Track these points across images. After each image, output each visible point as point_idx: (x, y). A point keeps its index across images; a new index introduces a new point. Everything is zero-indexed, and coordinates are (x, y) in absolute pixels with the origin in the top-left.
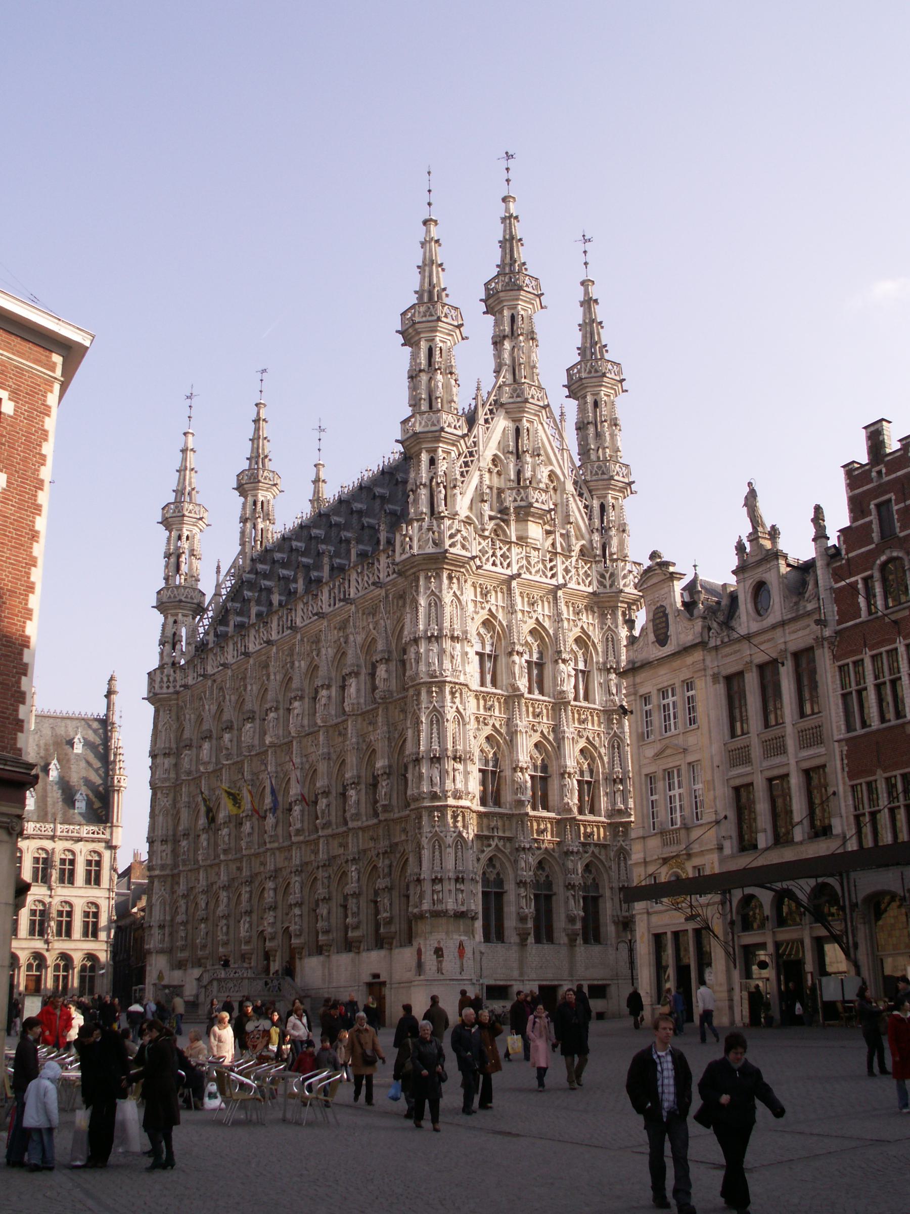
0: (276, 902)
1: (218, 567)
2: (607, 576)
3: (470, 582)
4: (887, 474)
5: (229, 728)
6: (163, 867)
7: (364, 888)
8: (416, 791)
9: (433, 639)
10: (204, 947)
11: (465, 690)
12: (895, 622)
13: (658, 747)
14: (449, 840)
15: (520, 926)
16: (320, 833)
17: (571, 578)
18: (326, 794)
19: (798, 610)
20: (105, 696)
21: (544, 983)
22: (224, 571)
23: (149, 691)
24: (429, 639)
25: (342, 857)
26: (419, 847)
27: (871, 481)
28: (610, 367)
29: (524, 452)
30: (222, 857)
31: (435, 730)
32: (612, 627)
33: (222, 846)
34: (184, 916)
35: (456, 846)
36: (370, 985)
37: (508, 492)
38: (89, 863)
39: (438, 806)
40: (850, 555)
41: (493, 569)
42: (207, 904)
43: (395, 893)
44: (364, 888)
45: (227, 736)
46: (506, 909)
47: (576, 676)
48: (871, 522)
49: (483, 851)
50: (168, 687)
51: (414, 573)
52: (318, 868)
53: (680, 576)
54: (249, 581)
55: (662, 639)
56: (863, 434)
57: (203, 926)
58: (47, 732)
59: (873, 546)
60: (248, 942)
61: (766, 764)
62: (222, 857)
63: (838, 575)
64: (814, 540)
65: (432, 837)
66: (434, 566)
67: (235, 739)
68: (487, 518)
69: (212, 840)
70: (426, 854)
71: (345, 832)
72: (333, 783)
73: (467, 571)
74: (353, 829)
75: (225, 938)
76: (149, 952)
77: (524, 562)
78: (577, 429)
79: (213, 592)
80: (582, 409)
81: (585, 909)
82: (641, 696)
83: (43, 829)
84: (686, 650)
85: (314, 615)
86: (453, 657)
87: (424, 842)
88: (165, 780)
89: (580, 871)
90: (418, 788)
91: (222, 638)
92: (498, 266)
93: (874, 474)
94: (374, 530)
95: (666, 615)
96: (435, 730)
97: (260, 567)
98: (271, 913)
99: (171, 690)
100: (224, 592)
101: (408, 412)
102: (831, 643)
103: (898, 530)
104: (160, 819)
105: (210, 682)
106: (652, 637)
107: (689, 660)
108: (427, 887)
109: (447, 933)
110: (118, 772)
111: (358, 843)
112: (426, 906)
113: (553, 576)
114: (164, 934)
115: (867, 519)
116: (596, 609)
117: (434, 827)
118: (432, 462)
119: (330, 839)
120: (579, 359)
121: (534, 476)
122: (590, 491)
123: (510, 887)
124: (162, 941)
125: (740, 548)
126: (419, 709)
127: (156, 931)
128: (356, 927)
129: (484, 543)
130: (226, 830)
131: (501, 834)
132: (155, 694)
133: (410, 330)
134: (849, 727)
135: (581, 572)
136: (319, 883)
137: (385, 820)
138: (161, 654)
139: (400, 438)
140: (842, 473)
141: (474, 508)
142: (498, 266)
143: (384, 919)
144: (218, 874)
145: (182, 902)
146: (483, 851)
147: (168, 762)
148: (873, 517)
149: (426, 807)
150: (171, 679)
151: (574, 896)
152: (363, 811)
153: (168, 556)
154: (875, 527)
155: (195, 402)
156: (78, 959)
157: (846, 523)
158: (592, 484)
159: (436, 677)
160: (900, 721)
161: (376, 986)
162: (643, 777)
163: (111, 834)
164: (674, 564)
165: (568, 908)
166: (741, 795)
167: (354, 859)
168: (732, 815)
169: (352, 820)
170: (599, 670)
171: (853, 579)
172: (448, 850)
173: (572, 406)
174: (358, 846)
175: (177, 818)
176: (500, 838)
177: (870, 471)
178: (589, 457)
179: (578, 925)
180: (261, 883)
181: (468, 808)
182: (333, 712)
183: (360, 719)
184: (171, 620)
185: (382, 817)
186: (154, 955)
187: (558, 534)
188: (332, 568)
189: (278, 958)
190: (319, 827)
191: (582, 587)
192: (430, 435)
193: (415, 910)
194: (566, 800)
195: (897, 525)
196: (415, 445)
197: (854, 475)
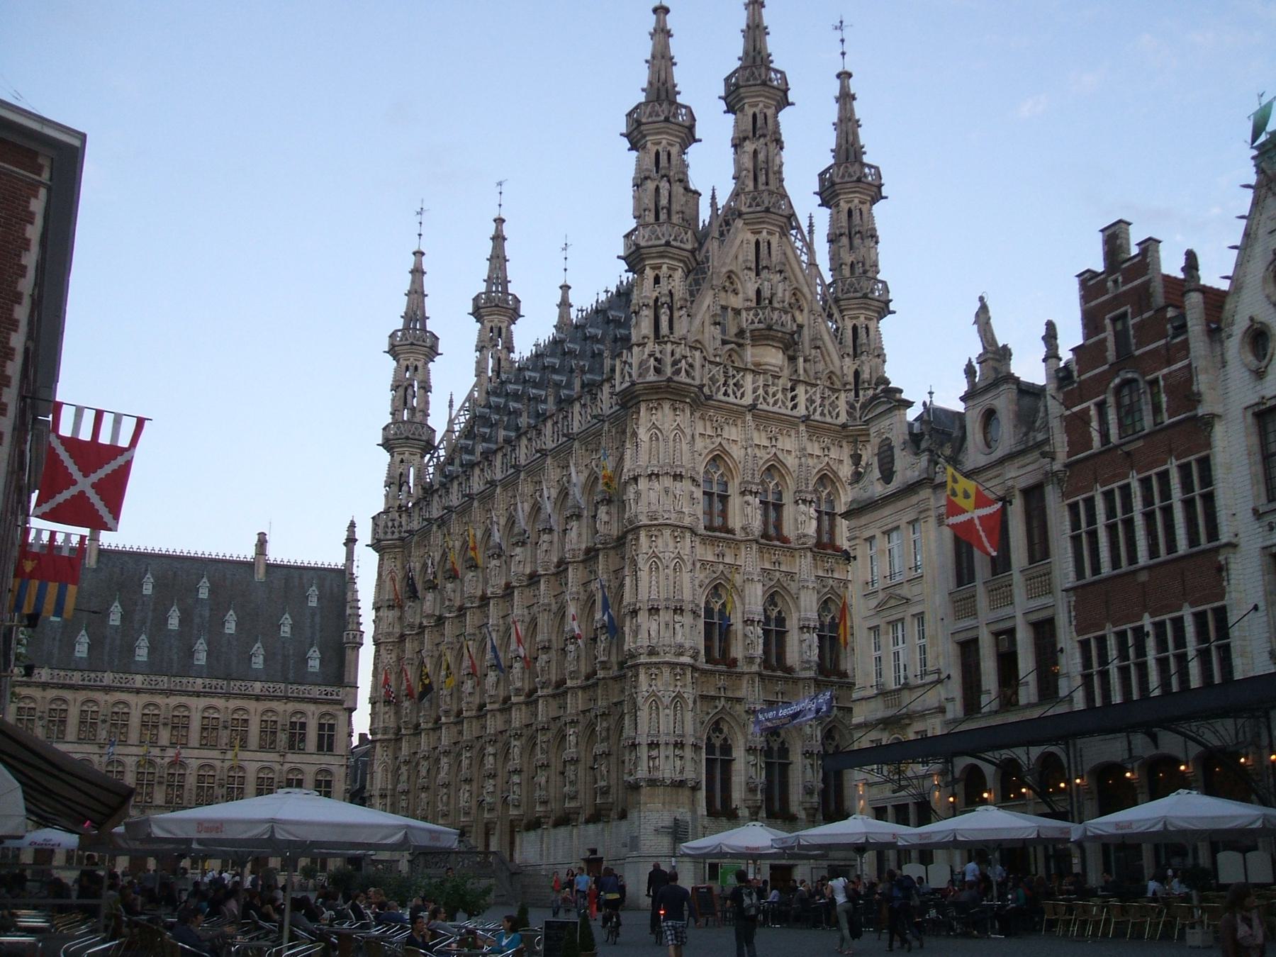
0: (495, 769)
1: (451, 401)
2: (858, 405)
3: (697, 415)
4: (1124, 283)
5: (453, 576)
6: (385, 730)
7: (583, 754)
8: (633, 645)
11: (688, 535)
12: (1128, 454)
13: (881, 595)
14: (667, 701)
15: (750, 796)
16: (539, 693)
17: (815, 410)
18: (546, 649)
19: (1027, 442)
21: (777, 862)
22: (457, 406)
23: (373, 538)
24: (650, 476)
26: (635, 708)
27: (1106, 292)
28: (867, 170)
33: (444, 707)
35: (675, 707)
36: (587, 861)
37: (744, 314)
38: (321, 727)
40: (1083, 377)
41: (726, 399)
43: (613, 759)
44: (583, 754)
46: (734, 779)
47: (819, 520)
48: (1105, 340)
49: (708, 714)
50: (393, 533)
53: (909, 404)
54: (482, 417)
55: (887, 476)
56: (1099, 238)
57: (423, 795)
59: (1106, 367)
60: (467, 814)
61: (993, 616)
63: (1068, 403)
64: (1044, 360)
68: (719, 342)
70: (643, 715)
72: (554, 638)
73: (693, 400)
77: (761, 391)
78: (830, 241)
79: (445, 428)
80: (834, 221)
81: (824, 780)
82: (866, 540)
84: (911, 489)
85: (537, 451)
87: (640, 700)
88: (389, 634)
89: (819, 738)
90: (635, 642)
91: (451, 478)
92: (740, 59)
93: (1110, 284)
94: (600, 354)
95: (891, 448)
97: (493, 399)
99: (396, 536)
100: (457, 428)
101: (633, 224)
102: (1060, 481)
103: (1133, 348)
105: (435, 528)
106: (877, 473)
107: (914, 499)
108: (644, 752)
109: (664, 804)
112: (642, 772)
113: (795, 407)
115: (1102, 336)
116: (844, 444)
118: (657, 280)
119: (550, 700)
120: (832, 161)
121: (773, 295)
122: (841, 311)
123: (739, 753)
125: (969, 371)
128: (573, 798)
129: (715, 370)
131: (730, 694)
132: (379, 541)
133: (635, 133)
134: (1080, 573)
135: (827, 402)
136: (538, 748)
138: (387, 496)
139: (622, 254)
140: (1075, 285)
141: (706, 330)
142: (740, 59)
143: (601, 788)
144: (439, 738)
145: (404, 769)
146: (708, 714)
148: (1109, 334)
149: (642, 664)
150: (396, 524)
151: (812, 765)
153: (395, 388)
154: (1111, 344)
157: (1079, 341)
158: (842, 303)
160: (1133, 568)
161: (593, 862)
162: (866, 631)
164: (901, 391)
165: (803, 775)
166: (968, 648)
167: (572, 722)
168: (956, 674)
169: (572, 679)
171: (1084, 405)
172: (667, 711)
173: (823, 218)
176: (728, 699)
177: (1105, 281)
178: (841, 274)
179: (816, 799)
180: (483, 749)
181: (689, 665)
183: (581, 567)
185: (601, 674)
187: (801, 360)
188: (559, 401)
189: (497, 832)
191: (828, 419)
192: (654, 250)
193: (631, 779)
194: (805, 657)
195: (1133, 341)
196: (639, 263)
197: (1089, 284)
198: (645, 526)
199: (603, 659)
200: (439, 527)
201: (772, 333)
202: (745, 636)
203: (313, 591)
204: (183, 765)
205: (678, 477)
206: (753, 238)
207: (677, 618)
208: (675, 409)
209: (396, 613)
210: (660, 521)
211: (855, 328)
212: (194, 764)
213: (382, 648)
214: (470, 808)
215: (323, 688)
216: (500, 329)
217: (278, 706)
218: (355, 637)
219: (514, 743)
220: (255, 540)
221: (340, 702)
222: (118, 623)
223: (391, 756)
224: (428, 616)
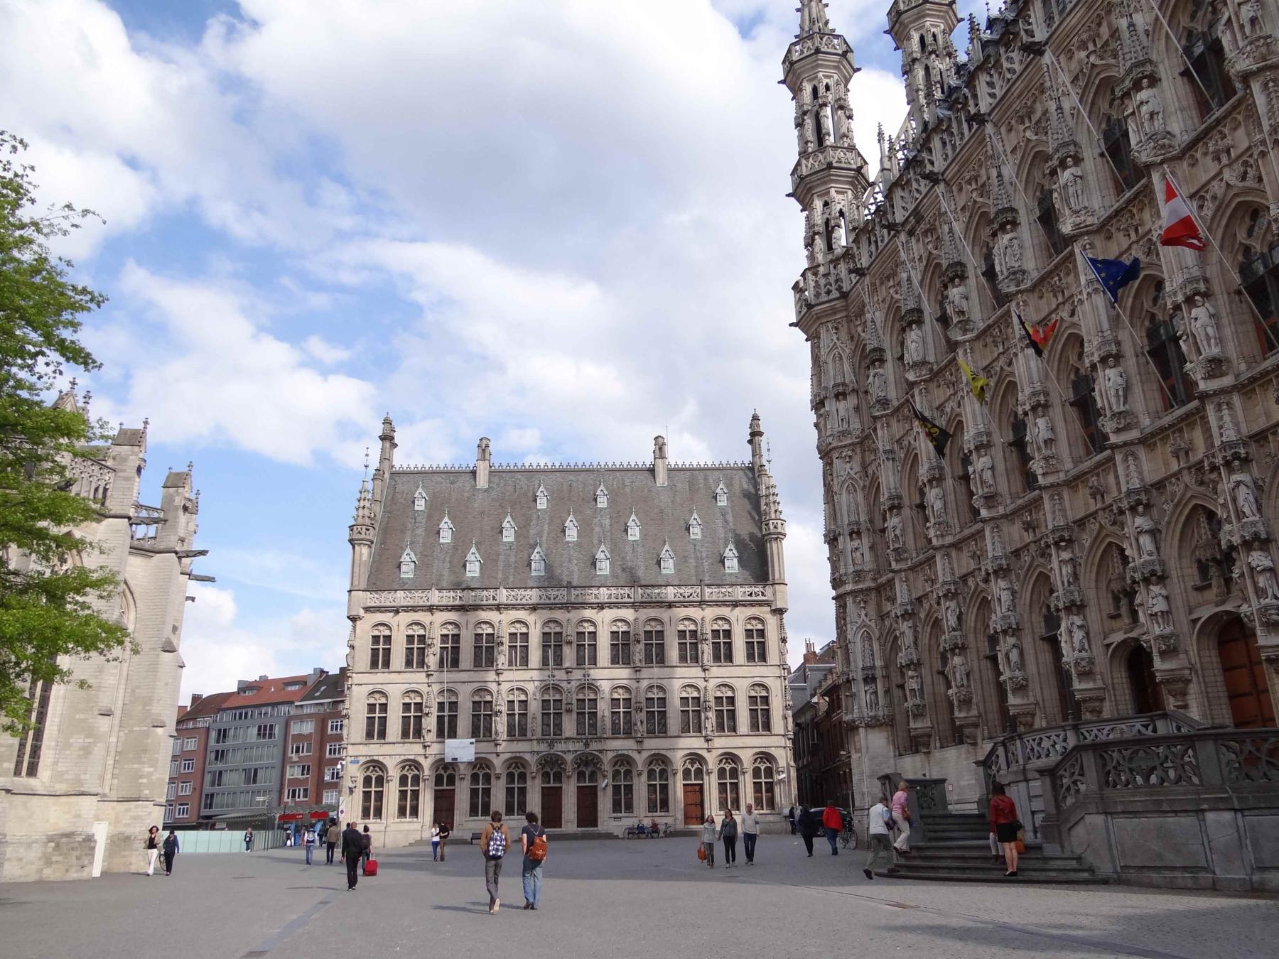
1: (880, 134)
6: (858, 575)
10: (966, 702)
20: (750, 442)
30: (984, 513)
34: (912, 650)
38: (749, 633)
42: (959, 618)
45: (955, 292)
57: (957, 660)
58: (682, 486)
75: (1017, 673)
76: (853, 728)
88: (844, 433)
98: (1155, 589)
104: (844, 499)
105: (903, 237)
110: (773, 516)
114: (876, 693)
124: (874, 705)
127: (860, 688)
147: (843, 407)
156: (747, 757)
163: (774, 594)
184: (818, 204)
186: (862, 731)
200: (911, 233)
203: (721, 489)
204: (593, 688)
209: (852, 401)
212: (605, 686)
213: (835, 455)
214: (1091, 661)
215: (748, 589)
216: (934, 36)
220: (651, 446)
222: (512, 539)
223: (873, 614)
224: (916, 365)
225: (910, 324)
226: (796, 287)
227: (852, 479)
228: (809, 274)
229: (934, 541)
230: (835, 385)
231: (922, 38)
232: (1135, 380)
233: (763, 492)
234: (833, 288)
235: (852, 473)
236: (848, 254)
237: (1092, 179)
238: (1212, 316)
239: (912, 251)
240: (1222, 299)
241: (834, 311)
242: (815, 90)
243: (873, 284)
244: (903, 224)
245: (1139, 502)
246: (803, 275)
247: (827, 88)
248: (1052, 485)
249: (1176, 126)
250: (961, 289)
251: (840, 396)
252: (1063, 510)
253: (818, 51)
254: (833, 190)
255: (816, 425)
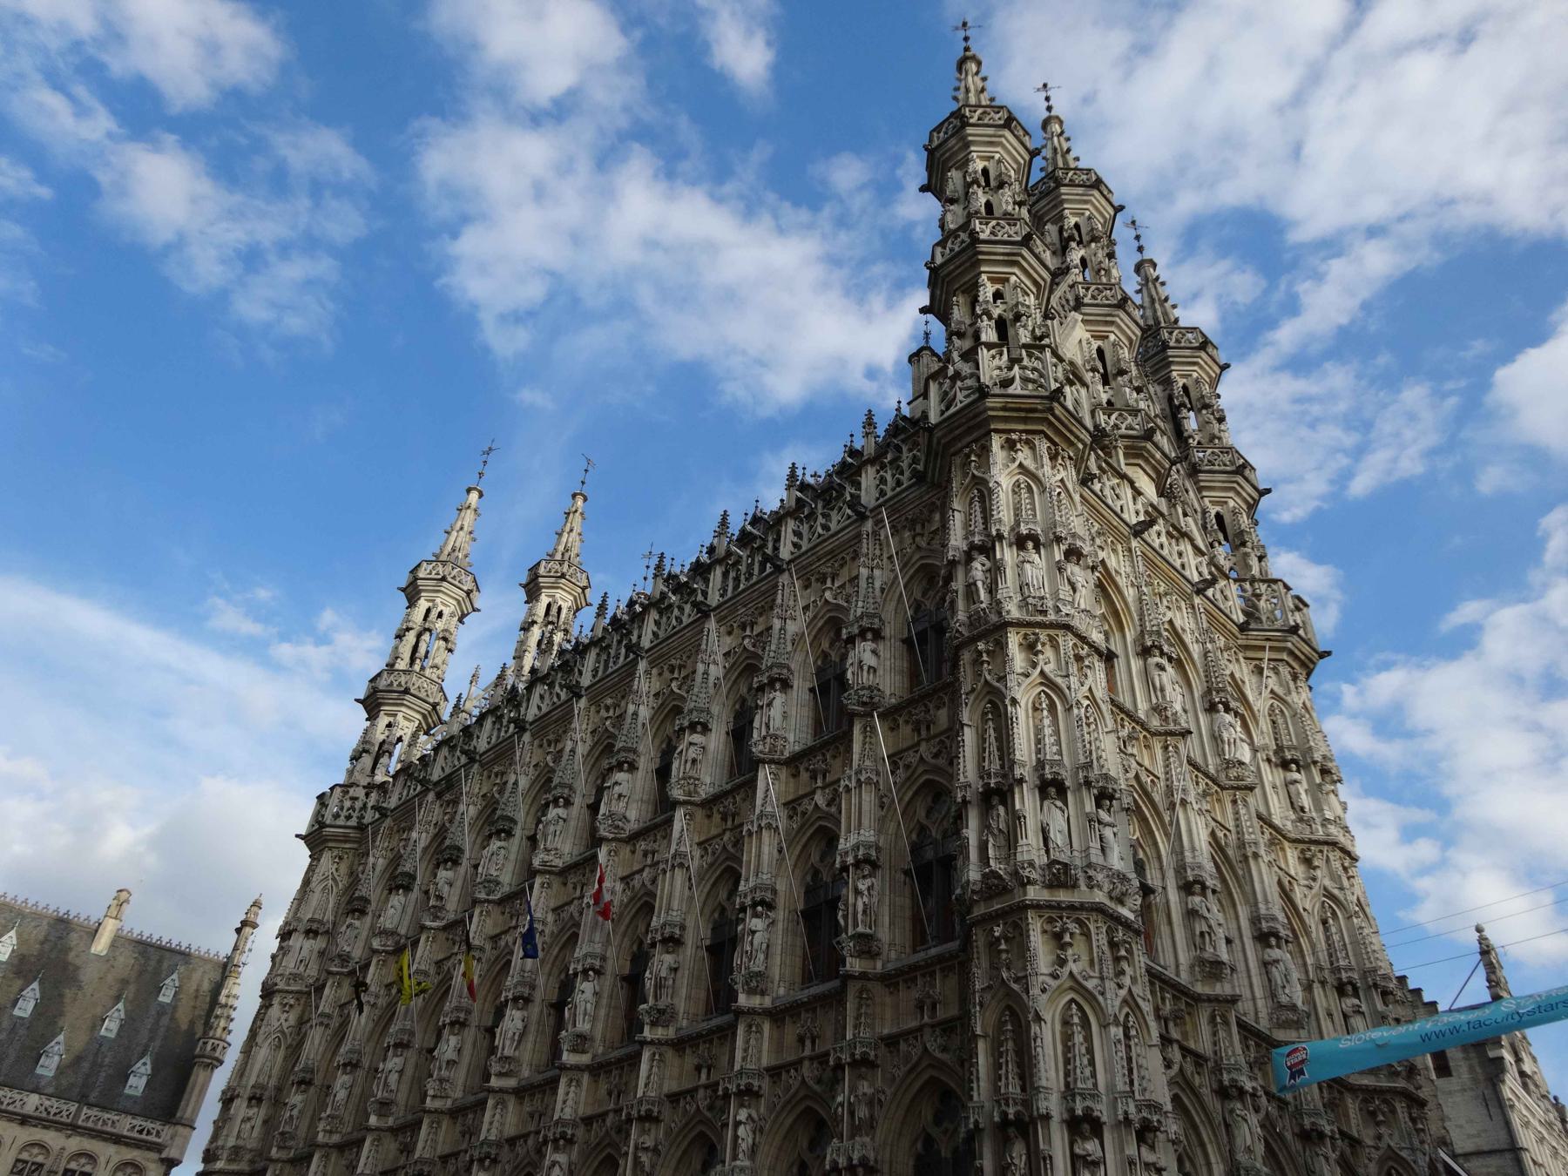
6: (236, 1152)
9: (1030, 545)
16: (647, 1033)
18: (673, 942)
20: (238, 931)
25: (701, 1093)
29: (1122, 372)
31: (1047, 722)
32: (1280, 691)
39: (1072, 907)
45: (443, 874)
50: (349, 817)
51: (975, 441)
52: (623, 1130)
62: (373, 1120)
65: (1060, 991)
66: (1022, 427)
67: (459, 883)
69: (357, 1090)
70: (1047, 1040)
71: (720, 1029)
74: (752, 1012)
83: (53, 1111)
86: (1074, 590)
88: (295, 977)
96: (1047, 722)
99: (353, 822)
104: (262, 1053)
105: (431, 796)
108: (1057, 1143)
111: (760, 1052)
117: (1062, 962)
119: (669, 1054)
122: (1200, 489)
126: (1002, 679)
130: (396, 1060)
137: (864, 976)
138: (351, 772)
149: (1037, 906)
150: (358, 805)
152: (776, 972)
155: (491, 458)
158: (1202, 476)
159: (1044, 613)
170: (1269, 760)
174: (759, 1059)
175: (295, 1050)
182: (708, 780)
190: (647, 1020)
198: (1019, 624)
199: (860, 929)
200: (439, 796)
201: (1149, 446)
202: (1191, 914)
205: (1073, 554)
206: (1095, 344)
207: (1103, 815)
208: (1053, 458)
209: (319, 943)
210: (1052, 617)
211: (1219, 517)
213: (276, 1000)
215: (138, 1122)
216: (560, 609)
217: (52, 1138)
218: (214, 1049)
219: (551, 1156)
221: (158, 1148)
224: (384, 933)
225: (398, 888)
226: (321, 797)
227: (283, 1032)
228: (338, 790)
229: (321, 1138)
230: (311, 920)
231: (549, 606)
232: (533, 1028)
233: (222, 999)
234: (355, 815)
235: (285, 1025)
236: (382, 787)
237: (573, 823)
238: (596, 993)
239: (430, 812)
240: (608, 980)
241: (346, 839)
242: (428, 611)
243: (391, 828)
244: (437, 784)
245: (488, 1156)
246: (332, 789)
247: (440, 615)
248: (436, 1111)
249: (632, 814)
250: (450, 874)
251: (311, 933)
252: (435, 1141)
253: (444, 579)
254: (400, 715)
255: (273, 957)
